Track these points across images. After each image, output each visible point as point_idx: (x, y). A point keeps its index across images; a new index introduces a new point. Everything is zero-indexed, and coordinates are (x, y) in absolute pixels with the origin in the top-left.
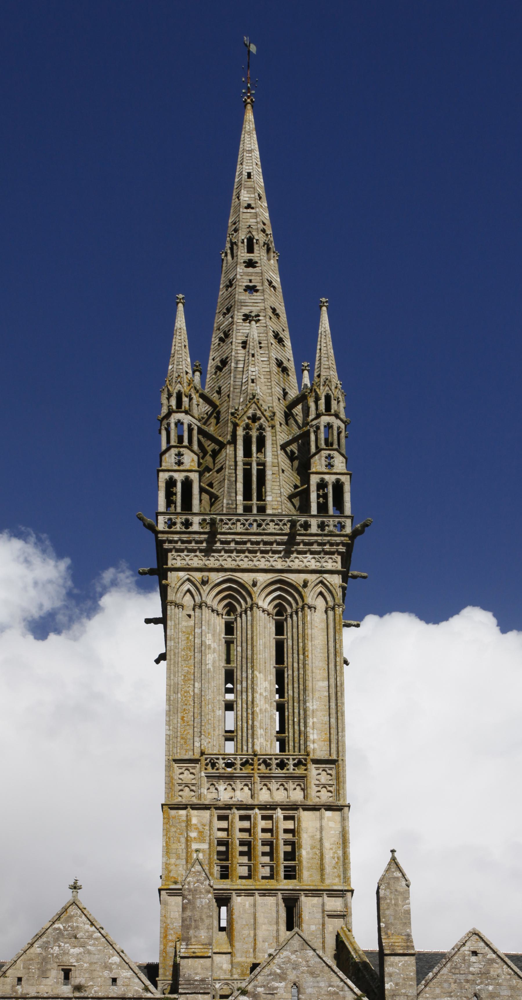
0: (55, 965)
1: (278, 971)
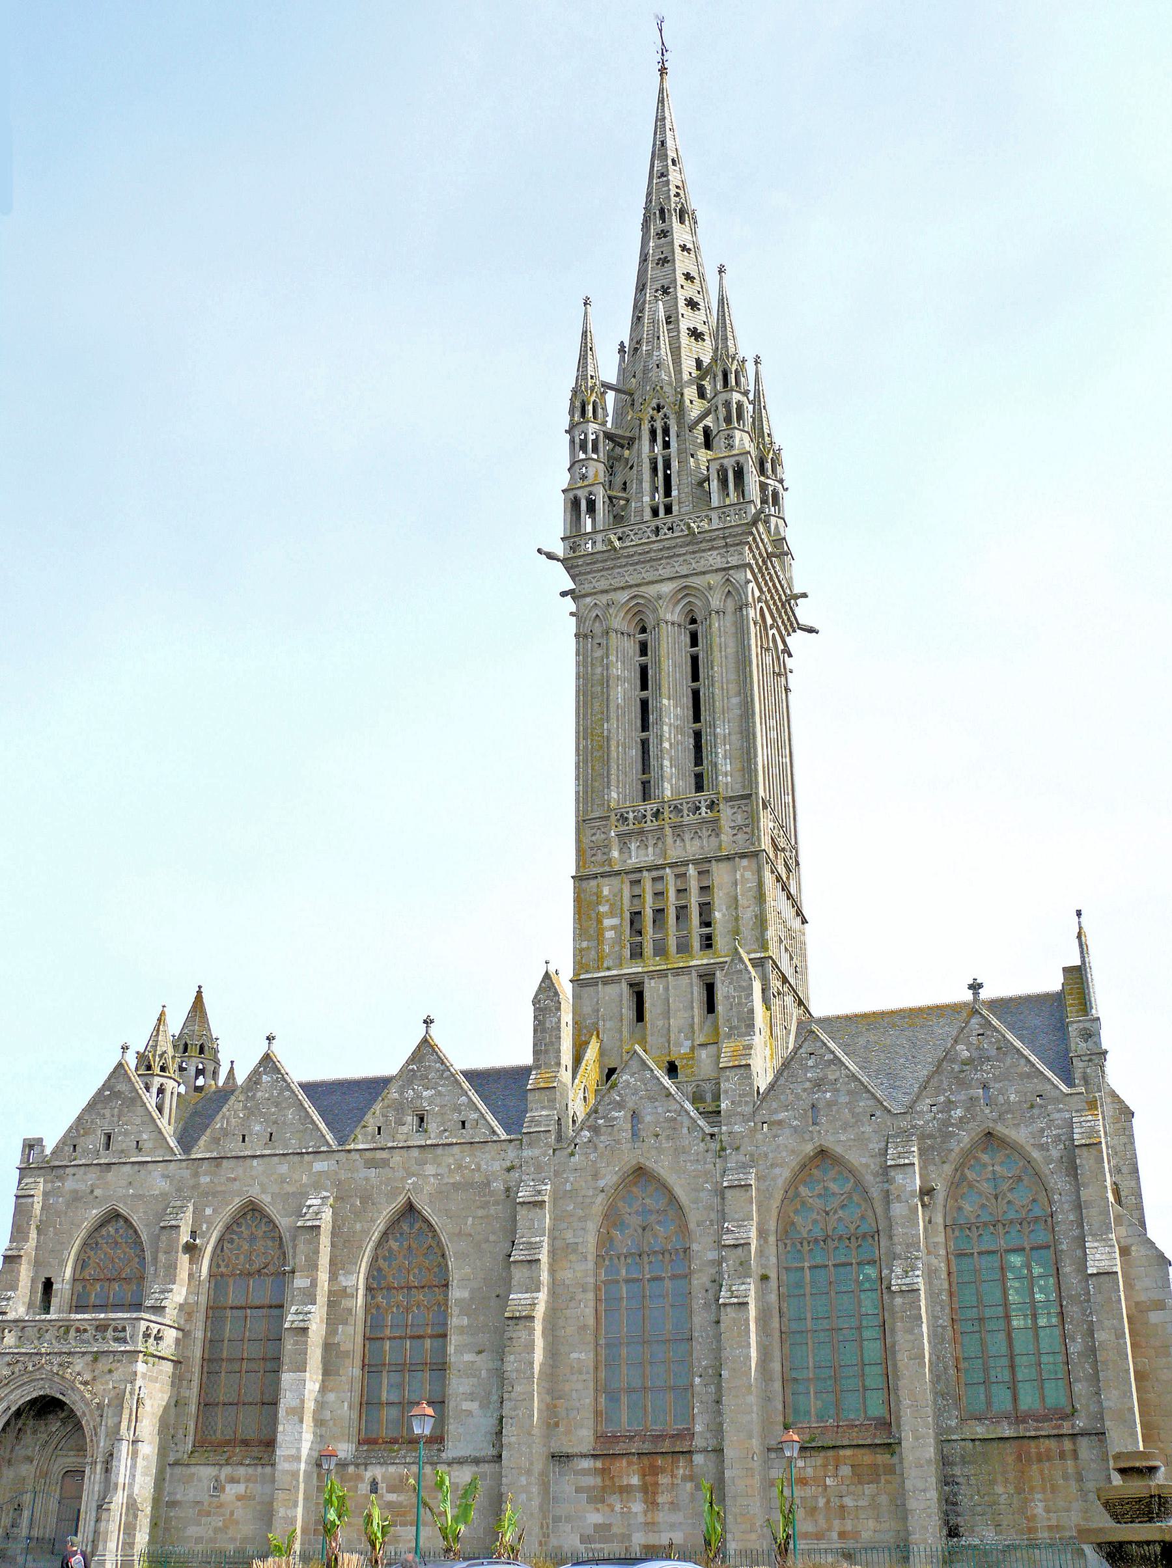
0: (410, 1112)
1: (618, 1098)
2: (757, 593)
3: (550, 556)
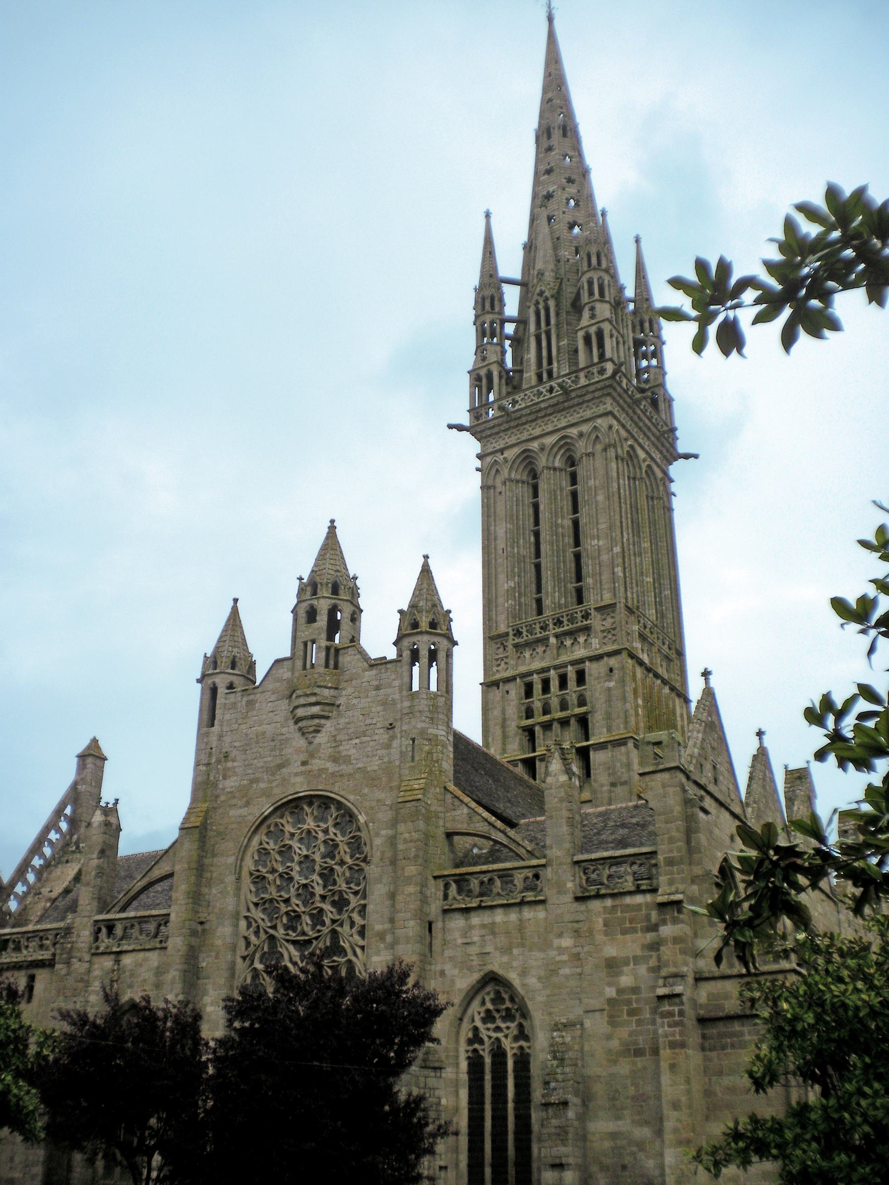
2: (623, 433)
3: (460, 428)
